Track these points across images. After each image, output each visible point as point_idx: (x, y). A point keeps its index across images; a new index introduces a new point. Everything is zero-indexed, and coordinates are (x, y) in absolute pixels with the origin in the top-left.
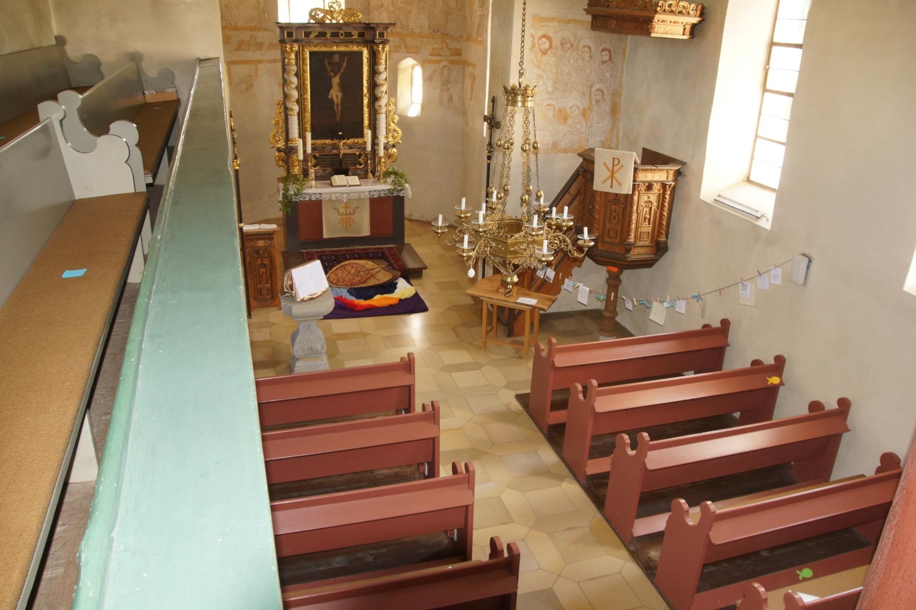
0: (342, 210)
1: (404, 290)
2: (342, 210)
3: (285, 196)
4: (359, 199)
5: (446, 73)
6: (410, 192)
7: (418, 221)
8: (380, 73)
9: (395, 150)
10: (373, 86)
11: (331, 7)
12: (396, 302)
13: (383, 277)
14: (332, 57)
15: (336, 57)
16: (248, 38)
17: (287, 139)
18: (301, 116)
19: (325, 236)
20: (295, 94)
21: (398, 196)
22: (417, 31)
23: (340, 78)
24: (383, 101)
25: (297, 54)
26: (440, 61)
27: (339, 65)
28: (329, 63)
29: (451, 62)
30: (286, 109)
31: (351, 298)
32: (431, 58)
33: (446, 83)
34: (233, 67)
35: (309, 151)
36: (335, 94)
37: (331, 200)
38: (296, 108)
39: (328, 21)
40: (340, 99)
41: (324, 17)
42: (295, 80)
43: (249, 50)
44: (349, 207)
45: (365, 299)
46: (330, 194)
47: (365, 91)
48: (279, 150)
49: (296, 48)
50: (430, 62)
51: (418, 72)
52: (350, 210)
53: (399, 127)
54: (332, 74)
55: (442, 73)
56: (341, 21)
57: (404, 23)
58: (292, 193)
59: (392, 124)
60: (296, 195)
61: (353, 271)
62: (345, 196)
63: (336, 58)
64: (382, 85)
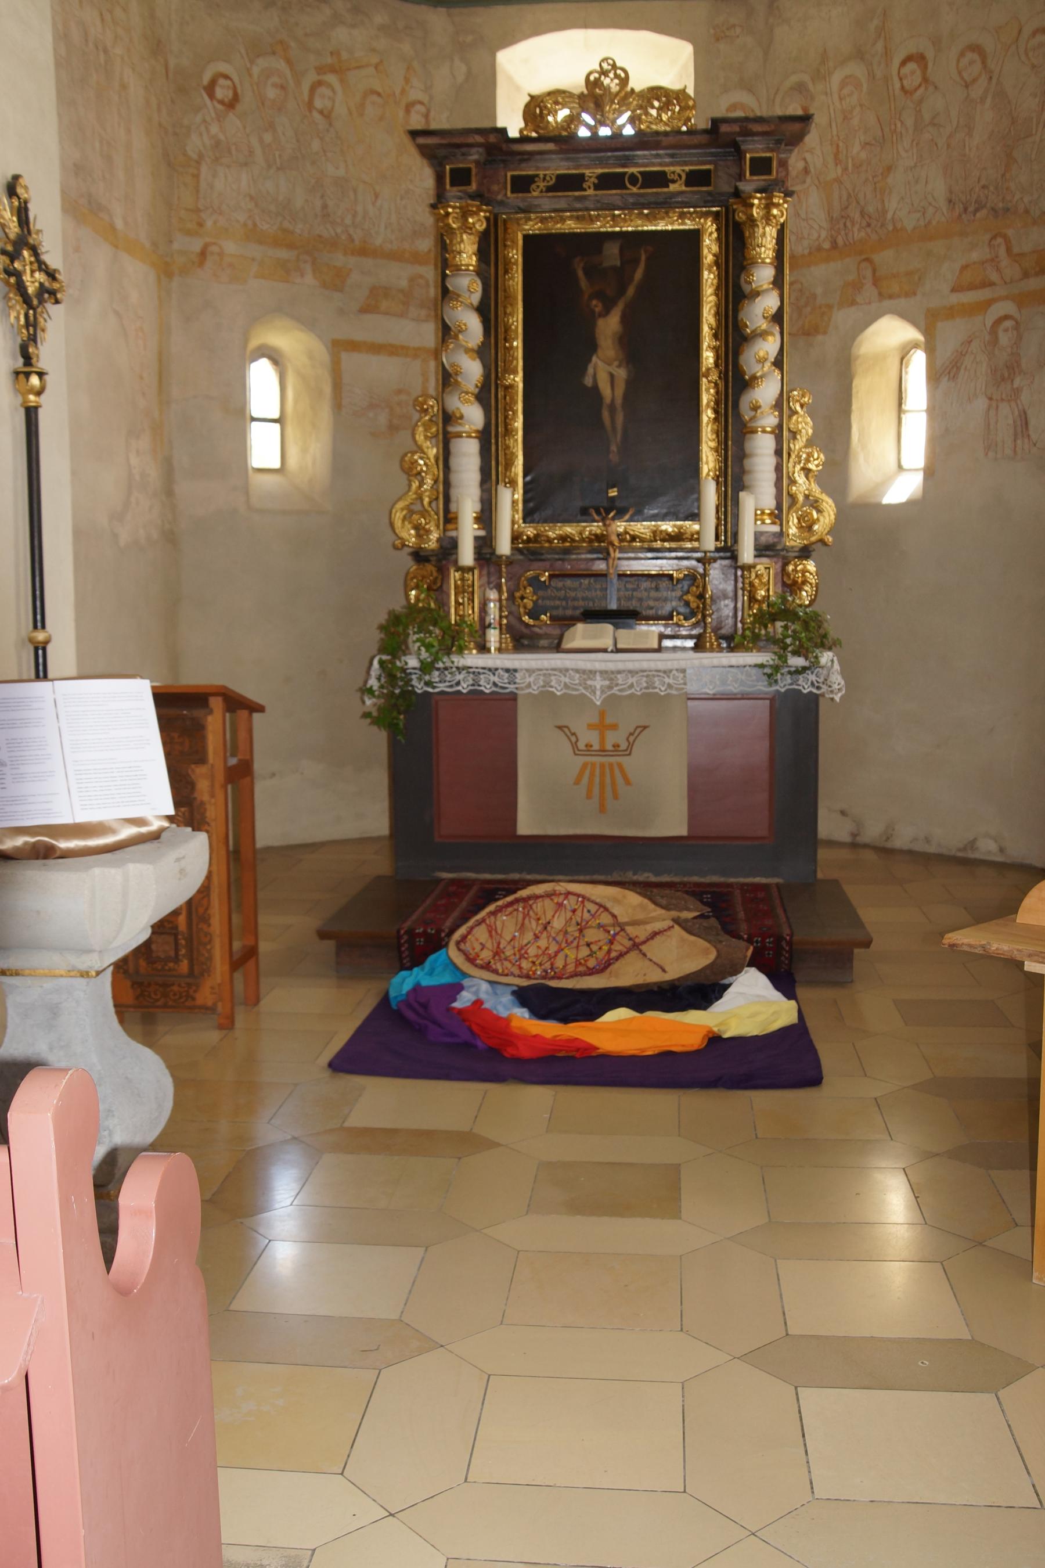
0: (588, 737)
1: (752, 1005)
2: (588, 737)
3: (390, 673)
4: (651, 700)
5: (1004, 339)
6: (837, 680)
7: (910, 852)
8: (757, 294)
9: (811, 566)
10: (734, 337)
11: (597, 83)
12: (693, 1042)
13: (680, 955)
14: (599, 251)
15: (612, 253)
16: (404, 283)
17: (450, 519)
18: (489, 440)
19: (526, 826)
20: (472, 370)
21: (794, 695)
22: (909, 223)
23: (624, 319)
24: (766, 392)
25: (489, 248)
26: (989, 303)
27: (622, 276)
28: (587, 273)
29: (1022, 300)
30: (448, 418)
31: (521, 1018)
32: (955, 299)
33: (1006, 374)
34: (350, 360)
35: (504, 546)
36: (606, 372)
37: (546, 697)
38: (474, 415)
39: (583, 133)
40: (620, 391)
41: (573, 120)
42: (472, 325)
43: (402, 315)
44: (615, 729)
45: (565, 1020)
46: (547, 673)
47: (708, 357)
48: (419, 556)
49: (478, 222)
50: (951, 313)
51: (919, 360)
52: (611, 738)
53: (824, 490)
54: (597, 305)
55: (995, 340)
56: (629, 131)
57: (870, 209)
58: (413, 662)
59: (800, 478)
60: (426, 668)
61: (558, 924)
62: (598, 683)
63: (612, 253)
64: (763, 334)
